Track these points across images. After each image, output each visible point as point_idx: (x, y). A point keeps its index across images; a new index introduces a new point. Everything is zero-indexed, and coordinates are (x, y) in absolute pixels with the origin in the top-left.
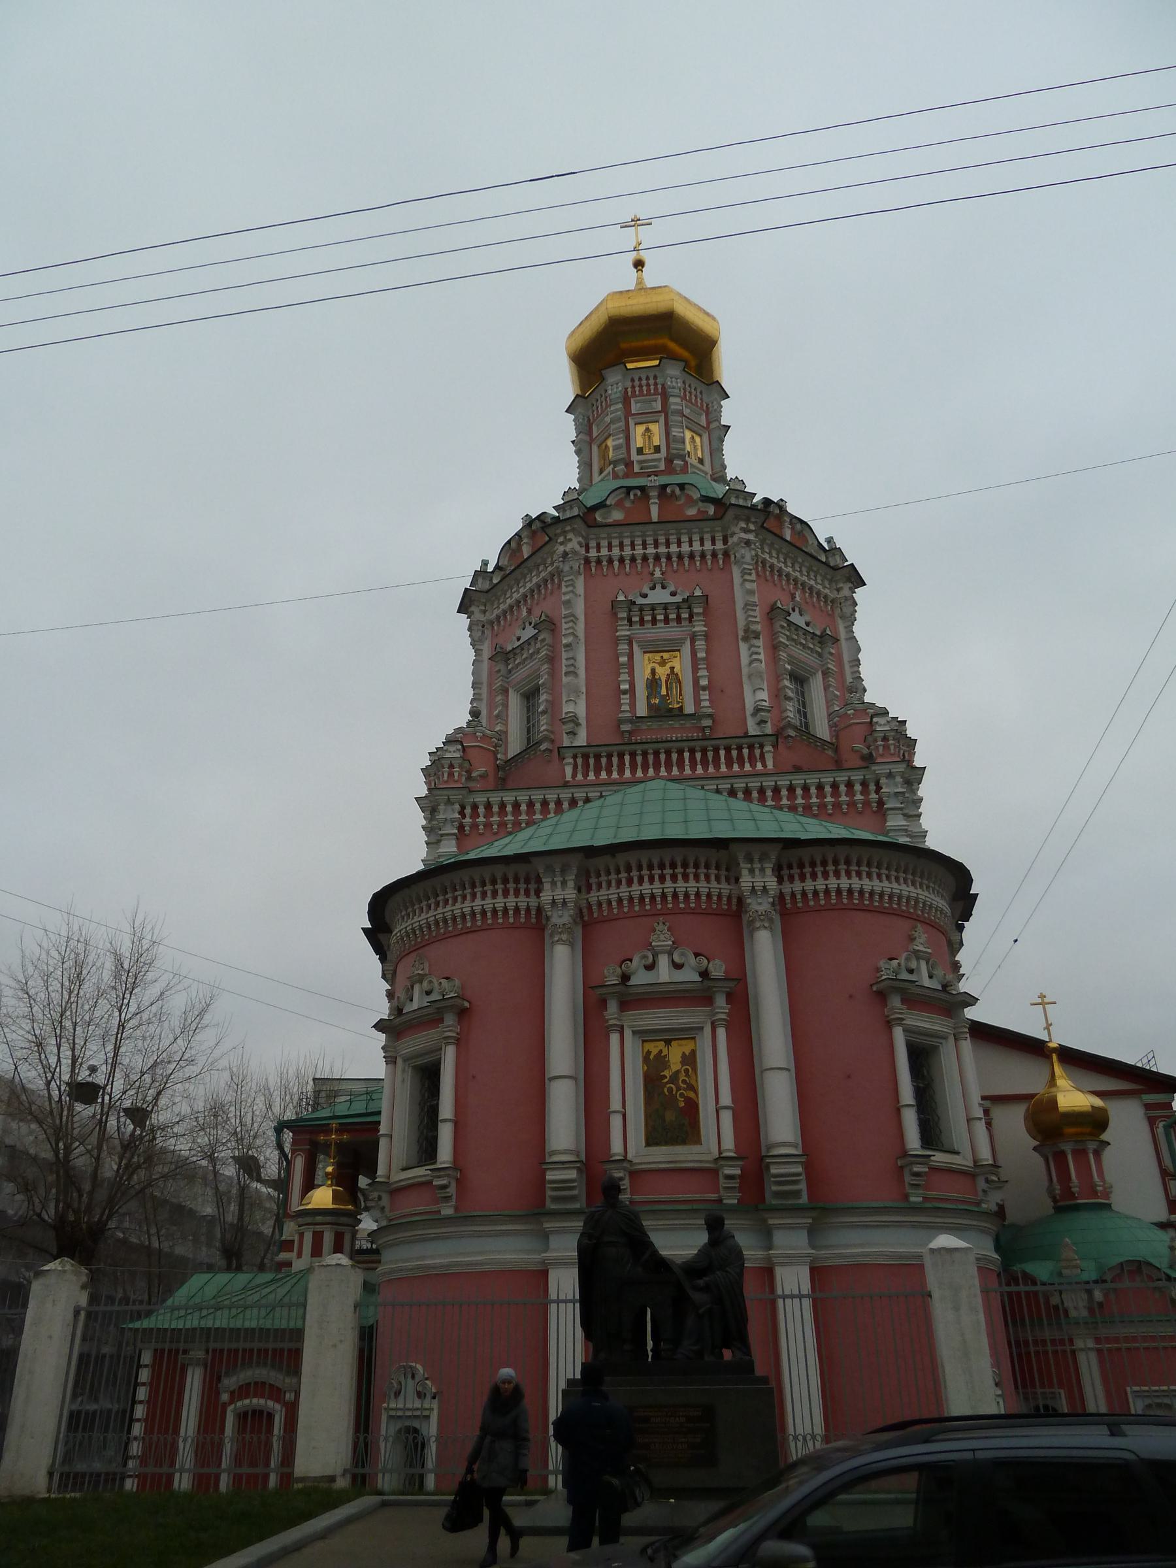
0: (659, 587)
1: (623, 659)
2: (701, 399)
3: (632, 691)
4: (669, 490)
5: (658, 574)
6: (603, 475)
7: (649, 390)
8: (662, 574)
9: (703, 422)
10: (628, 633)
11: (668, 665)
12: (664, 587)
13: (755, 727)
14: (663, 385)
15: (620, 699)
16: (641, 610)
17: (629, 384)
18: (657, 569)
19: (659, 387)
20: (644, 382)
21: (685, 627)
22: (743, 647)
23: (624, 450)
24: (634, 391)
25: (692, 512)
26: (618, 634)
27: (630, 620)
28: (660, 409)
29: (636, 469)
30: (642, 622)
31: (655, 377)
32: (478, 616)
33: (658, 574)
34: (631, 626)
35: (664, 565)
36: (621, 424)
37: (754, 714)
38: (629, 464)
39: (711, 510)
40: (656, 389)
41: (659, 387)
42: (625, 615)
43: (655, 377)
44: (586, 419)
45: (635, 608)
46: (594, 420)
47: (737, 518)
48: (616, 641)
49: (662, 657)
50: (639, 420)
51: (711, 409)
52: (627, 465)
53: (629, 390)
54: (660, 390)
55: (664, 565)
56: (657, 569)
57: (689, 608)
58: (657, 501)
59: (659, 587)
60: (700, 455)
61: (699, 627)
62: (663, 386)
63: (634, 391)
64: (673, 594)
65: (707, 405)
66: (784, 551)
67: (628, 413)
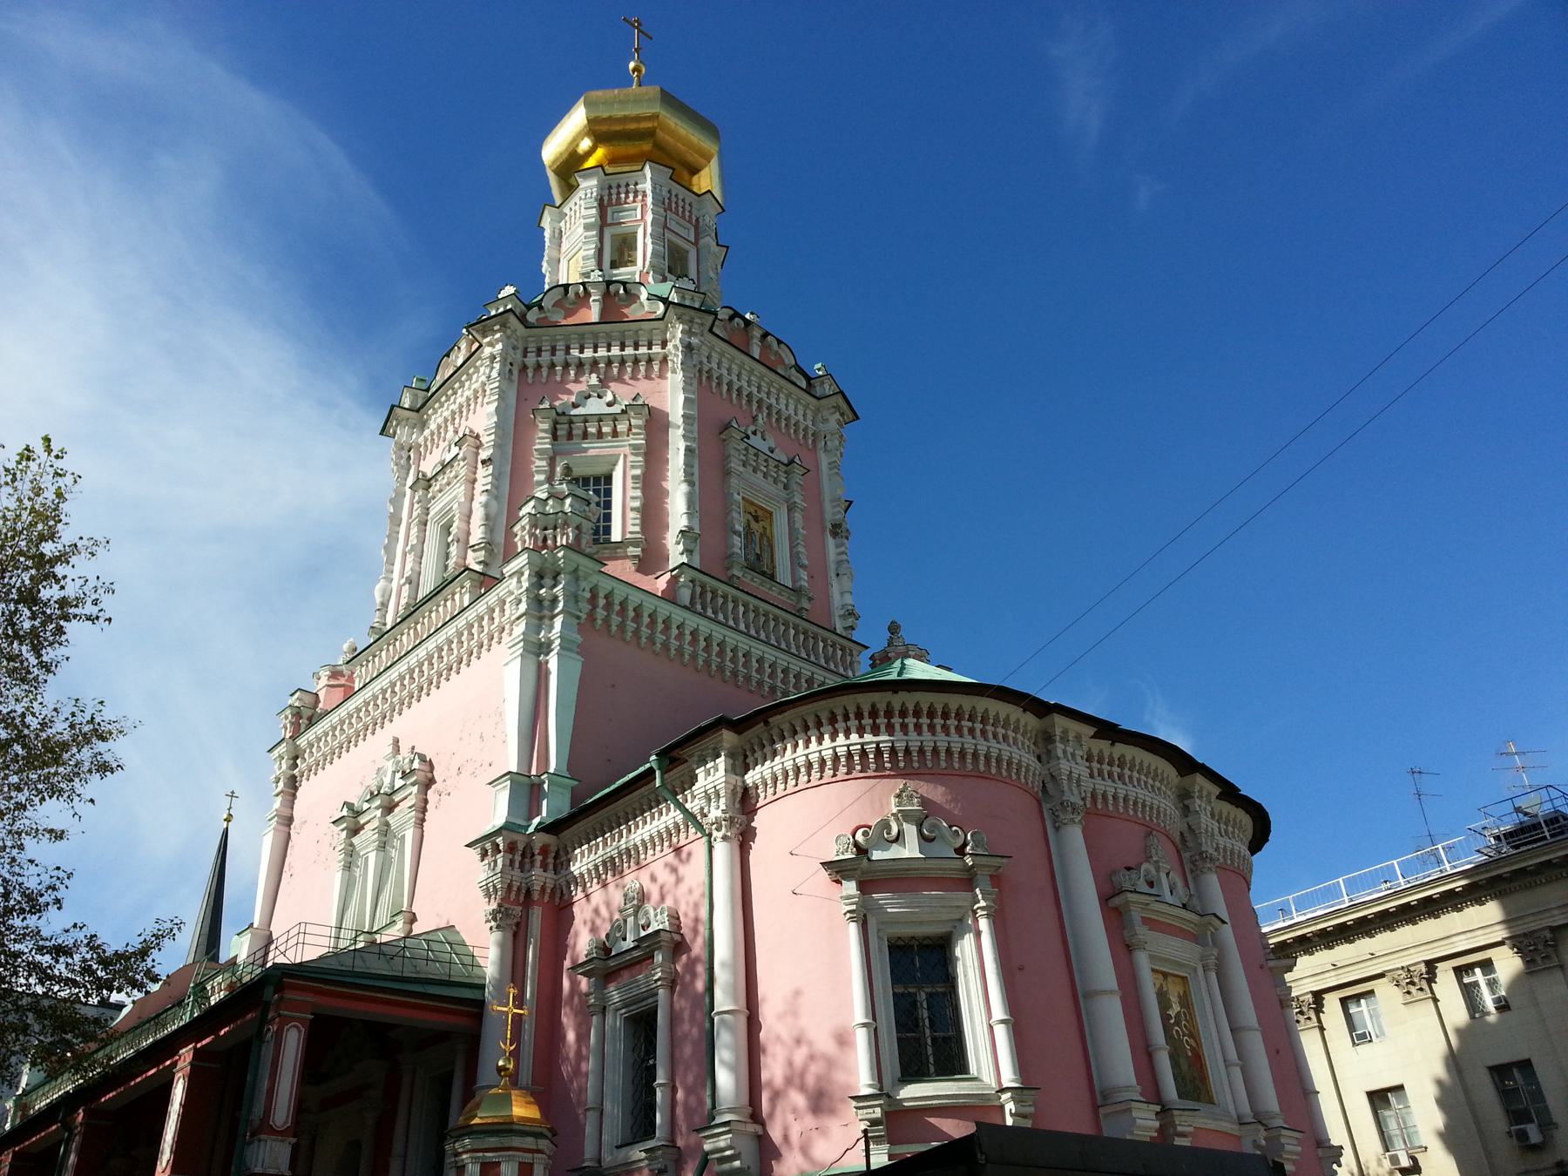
0: (759, 434)
11: (762, 523)
13: (842, 630)
19: (694, 219)
22: (831, 542)
33: (760, 421)
37: (843, 617)
39: (803, 384)
40: (690, 217)
41: (694, 219)
46: (610, 204)
47: (837, 408)
49: (756, 511)
55: (765, 414)
59: (759, 434)
62: (697, 220)
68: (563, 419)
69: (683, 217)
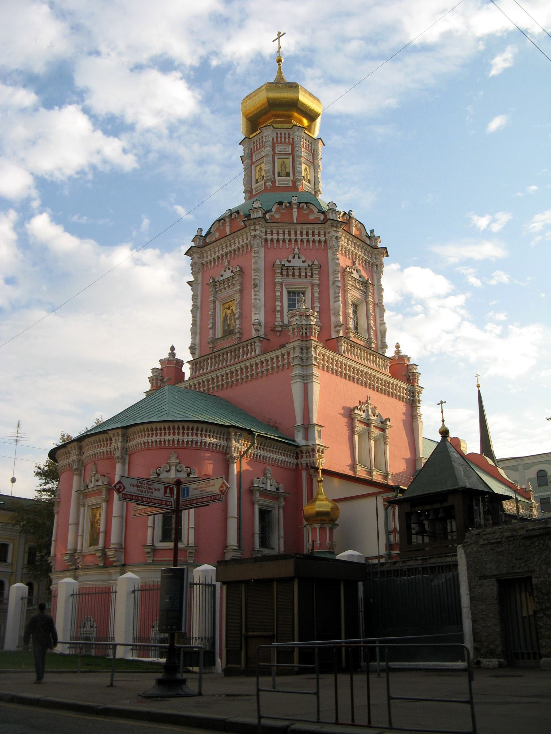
0: (296, 257)
1: (278, 294)
2: (311, 147)
3: (282, 311)
4: (301, 205)
5: (296, 250)
6: (258, 184)
7: (285, 140)
8: (299, 251)
9: (312, 161)
10: (281, 281)
12: (299, 258)
14: (293, 139)
15: (276, 316)
16: (287, 269)
17: (275, 136)
18: (296, 248)
19: (291, 140)
20: (283, 136)
21: (308, 280)
23: (271, 174)
24: (277, 140)
25: (312, 217)
26: (276, 281)
27: (281, 273)
28: (290, 152)
29: (277, 185)
30: (288, 275)
31: (289, 134)
32: (196, 259)
33: (296, 250)
34: (282, 277)
35: (299, 245)
36: (269, 158)
38: (274, 182)
39: (322, 217)
40: (289, 141)
41: (291, 140)
42: (280, 271)
43: (289, 134)
44: (250, 150)
45: (284, 268)
46: (255, 151)
48: (274, 284)
50: (280, 157)
51: (316, 152)
52: (272, 182)
53: (275, 139)
54: (291, 142)
55: (299, 245)
56: (296, 248)
57: (311, 270)
58: (296, 210)
59: (296, 257)
60: (309, 178)
61: (316, 281)
62: (293, 140)
63: (277, 140)
64: (304, 262)
65: (314, 150)
66: (358, 243)
67: (274, 153)
68: (218, 284)
69: (285, 143)
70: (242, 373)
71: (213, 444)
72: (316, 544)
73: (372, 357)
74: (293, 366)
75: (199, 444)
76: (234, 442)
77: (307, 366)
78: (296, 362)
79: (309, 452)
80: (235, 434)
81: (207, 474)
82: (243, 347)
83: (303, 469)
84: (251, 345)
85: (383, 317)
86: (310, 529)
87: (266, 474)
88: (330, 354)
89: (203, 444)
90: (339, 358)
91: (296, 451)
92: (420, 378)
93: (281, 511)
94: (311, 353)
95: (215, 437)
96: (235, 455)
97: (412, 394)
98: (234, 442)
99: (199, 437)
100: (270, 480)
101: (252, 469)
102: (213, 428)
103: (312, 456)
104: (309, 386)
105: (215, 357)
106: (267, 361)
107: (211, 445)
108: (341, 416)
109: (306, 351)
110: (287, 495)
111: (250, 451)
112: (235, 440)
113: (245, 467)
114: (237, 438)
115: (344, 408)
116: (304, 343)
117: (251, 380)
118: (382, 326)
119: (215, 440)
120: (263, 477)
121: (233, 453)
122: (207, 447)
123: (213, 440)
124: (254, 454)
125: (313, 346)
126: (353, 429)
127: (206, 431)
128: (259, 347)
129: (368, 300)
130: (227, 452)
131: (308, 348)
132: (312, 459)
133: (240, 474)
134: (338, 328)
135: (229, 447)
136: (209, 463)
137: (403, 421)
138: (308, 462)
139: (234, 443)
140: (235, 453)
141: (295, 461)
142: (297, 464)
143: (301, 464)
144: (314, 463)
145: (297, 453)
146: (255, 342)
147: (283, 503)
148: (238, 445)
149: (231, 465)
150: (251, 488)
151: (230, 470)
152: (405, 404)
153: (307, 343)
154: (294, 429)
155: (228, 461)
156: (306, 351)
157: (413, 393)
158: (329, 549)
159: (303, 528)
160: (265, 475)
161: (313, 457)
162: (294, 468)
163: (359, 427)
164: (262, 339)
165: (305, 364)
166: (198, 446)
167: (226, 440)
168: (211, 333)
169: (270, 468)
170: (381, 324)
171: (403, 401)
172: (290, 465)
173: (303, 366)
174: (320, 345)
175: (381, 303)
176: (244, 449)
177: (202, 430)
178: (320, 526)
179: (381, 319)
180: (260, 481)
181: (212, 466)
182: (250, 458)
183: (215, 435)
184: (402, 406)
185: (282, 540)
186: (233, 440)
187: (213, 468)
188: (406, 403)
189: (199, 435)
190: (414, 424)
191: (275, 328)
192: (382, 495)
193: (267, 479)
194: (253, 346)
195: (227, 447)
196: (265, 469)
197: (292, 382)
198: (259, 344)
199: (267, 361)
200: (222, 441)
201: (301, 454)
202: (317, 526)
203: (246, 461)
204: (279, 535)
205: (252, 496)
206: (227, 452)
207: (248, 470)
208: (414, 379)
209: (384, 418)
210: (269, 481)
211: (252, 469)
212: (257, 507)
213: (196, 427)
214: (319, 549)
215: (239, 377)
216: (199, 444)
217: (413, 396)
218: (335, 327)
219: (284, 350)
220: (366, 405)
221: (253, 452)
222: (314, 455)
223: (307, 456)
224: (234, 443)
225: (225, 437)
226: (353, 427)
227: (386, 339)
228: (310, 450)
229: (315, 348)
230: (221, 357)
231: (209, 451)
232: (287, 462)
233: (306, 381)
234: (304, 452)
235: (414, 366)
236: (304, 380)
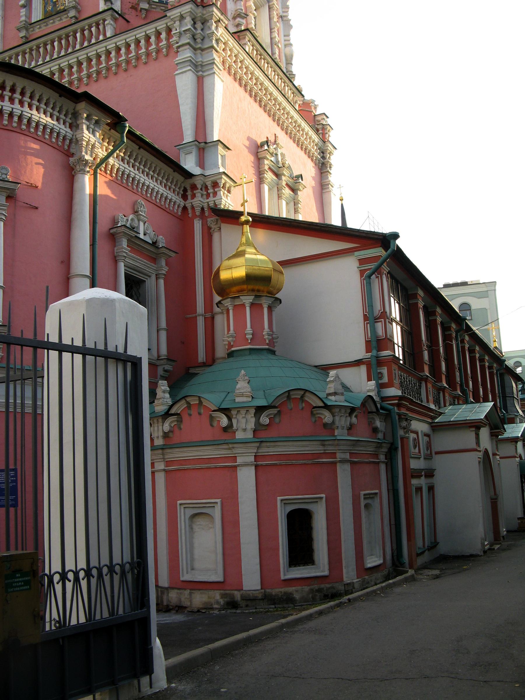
70: (80, 70)
71: (45, 127)
72: (246, 335)
73: (280, 81)
74: (178, 47)
75: (16, 119)
76: (86, 131)
77: (202, 50)
78: (186, 39)
79: (206, 188)
80: (88, 118)
81: (32, 182)
82: (83, 31)
83: (194, 216)
84: (98, 25)
85: (288, 36)
86: (230, 308)
87: (137, 212)
88: (234, 46)
89: (25, 121)
90: (244, 59)
91: (183, 185)
92: (332, 133)
93: (162, 282)
94: (210, 28)
95: (49, 114)
96: (87, 157)
97: (322, 154)
98: (86, 131)
99: (17, 105)
100: (144, 224)
101: (115, 197)
102: (47, 93)
103: (211, 195)
104: (207, 81)
105: (31, 50)
106: (128, 46)
107: (42, 127)
108: (246, 151)
109: (202, 27)
110: (173, 255)
111: (111, 161)
112: (88, 129)
113: (103, 190)
114: (92, 126)
115: (249, 139)
116: (200, 9)
117: (97, 81)
118: (288, 49)
119: (49, 119)
120: (131, 217)
121: (83, 153)
122: (32, 130)
123: (46, 119)
124: (118, 170)
125: (214, 18)
126: (260, 175)
127: (31, 98)
128: (112, 27)
129: (271, 4)
130: (72, 151)
131: (204, 22)
132: (211, 199)
133: (94, 197)
134: (238, 20)
135: (76, 141)
136: (37, 164)
137: (313, 187)
138: (205, 205)
139: (86, 134)
140: (86, 153)
141: (182, 204)
142: (185, 208)
143: (193, 208)
144: (216, 205)
145: (185, 190)
146: (104, 20)
147: (165, 270)
148: (93, 139)
149: (79, 177)
150: (112, 231)
151: (77, 186)
152: (314, 165)
153: (205, 12)
154: (179, 149)
155: (73, 169)
156: (202, 27)
157: (323, 153)
158: (268, 344)
159: (196, 317)
160: (136, 212)
161: (214, 196)
162: (180, 214)
163: (269, 176)
164: (117, 16)
165: (199, 46)
166: (15, 125)
167: (71, 127)
168: (24, 13)
169: (143, 203)
170: (286, 46)
171: (312, 160)
172: (173, 207)
173: (195, 49)
174: (224, 20)
175: (286, 16)
176: (101, 153)
177: (23, 94)
178: (254, 300)
179: (286, 38)
180: (127, 220)
181: (42, 170)
182: (111, 175)
183: (49, 109)
184: (312, 167)
185: (163, 335)
186: (85, 127)
187: (44, 175)
188: (316, 165)
189: (17, 101)
190: (325, 196)
191: (138, 5)
192: (356, 253)
193: (139, 220)
194: (101, 27)
195: (71, 140)
196: (135, 203)
197: (177, 72)
198: (112, 22)
199: (128, 46)
200: (62, 127)
201: (192, 191)
202: (247, 300)
203: (107, 180)
204: (157, 327)
205: (115, 246)
206: (72, 151)
207: (106, 196)
208: (324, 134)
209: (296, 173)
210: (142, 224)
211: (115, 197)
212: (122, 268)
213: (11, 84)
214: (250, 344)
215: (76, 76)
216: (16, 119)
217: (323, 158)
218: (234, 18)
219: (161, 25)
220: (275, 146)
221: (117, 166)
222: (215, 194)
223: (202, 195)
224: (86, 134)
225: (68, 120)
226: (260, 172)
227: (293, 67)
228: (209, 184)
229: (218, 21)
230: (41, 50)
231: (37, 139)
232: (171, 200)
233: (201, 73)
234: (199, 186)
235: (325, 117)
236: (197, 72)
